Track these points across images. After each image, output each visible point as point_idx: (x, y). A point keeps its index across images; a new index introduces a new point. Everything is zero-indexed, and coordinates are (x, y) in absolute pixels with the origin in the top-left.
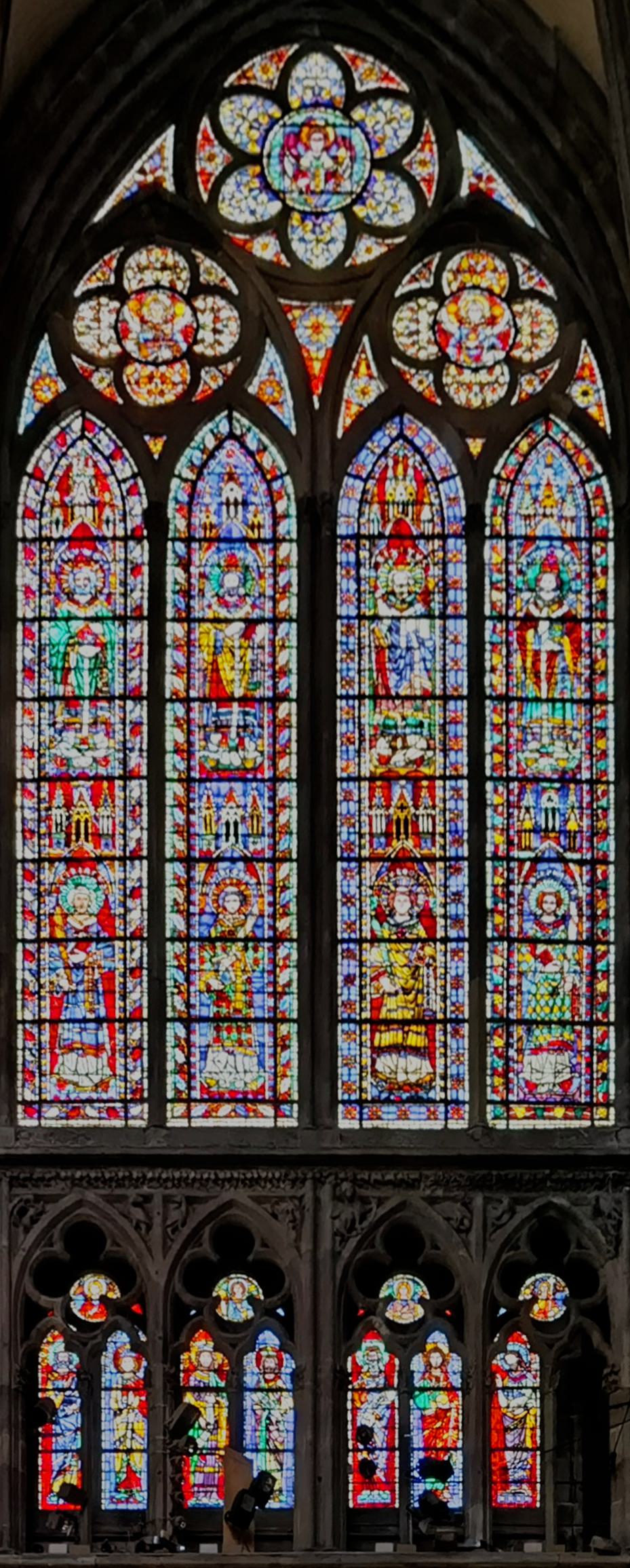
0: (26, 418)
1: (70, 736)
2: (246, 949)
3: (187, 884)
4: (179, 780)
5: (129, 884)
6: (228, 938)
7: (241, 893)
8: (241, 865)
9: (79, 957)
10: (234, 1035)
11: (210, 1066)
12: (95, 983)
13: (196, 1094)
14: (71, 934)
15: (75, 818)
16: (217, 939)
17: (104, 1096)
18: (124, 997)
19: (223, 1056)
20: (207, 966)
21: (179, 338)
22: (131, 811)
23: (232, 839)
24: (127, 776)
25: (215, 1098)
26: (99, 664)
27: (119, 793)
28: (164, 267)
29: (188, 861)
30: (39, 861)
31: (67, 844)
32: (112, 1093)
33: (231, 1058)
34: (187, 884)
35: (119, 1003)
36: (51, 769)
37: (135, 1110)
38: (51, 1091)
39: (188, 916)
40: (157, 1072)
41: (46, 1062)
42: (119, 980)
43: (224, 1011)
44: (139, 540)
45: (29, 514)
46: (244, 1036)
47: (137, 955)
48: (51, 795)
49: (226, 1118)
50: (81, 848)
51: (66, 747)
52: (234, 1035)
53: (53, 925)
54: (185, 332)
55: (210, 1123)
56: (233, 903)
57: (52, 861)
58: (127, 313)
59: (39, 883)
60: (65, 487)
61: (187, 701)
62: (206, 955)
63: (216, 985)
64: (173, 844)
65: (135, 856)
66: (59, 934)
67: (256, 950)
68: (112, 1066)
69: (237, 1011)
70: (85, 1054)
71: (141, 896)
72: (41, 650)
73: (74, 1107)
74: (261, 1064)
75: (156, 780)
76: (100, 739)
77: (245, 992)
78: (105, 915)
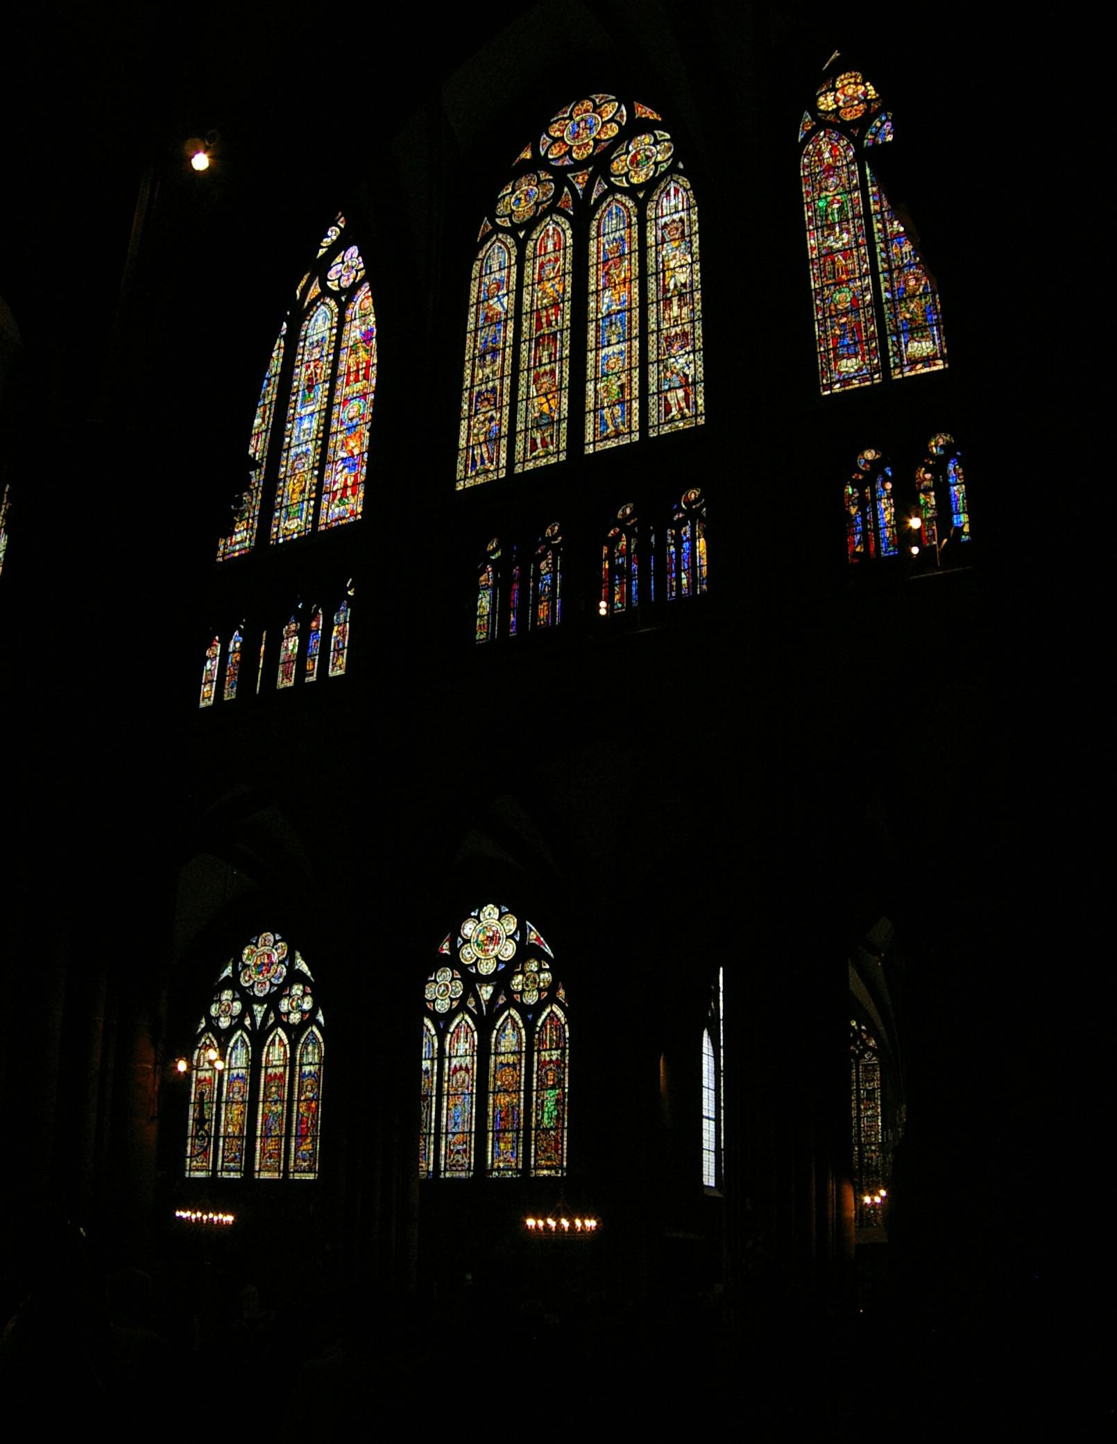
0: (800, 137)
1: (832, 238)
2: (920, 299)
3: (891, 280)
4: (882, 242)
5: (864, 286)
6: (912, 296)
7: (915, 278)
8: (914, 267)
9: (844, 320)
10: (920, 334)
11: (910, 350)
12: (852, 328)
13: (905, 363)
14: (839, 312)
15: (836, 267)
16: (906, 298)
17: (861, 373)
18: (866, 331)
19: (916, 344)
20: (904, 309)
21: (861, 96)
22: (861, 259)
23: (909, 258)
24: (858, 246)
25: (913, 362)
26: (841, 210)
27: (855, 253)
28: (851, 77)
29: (890, 271)
30: (822, 289)
31: (834, 277)
32: (865, 372)
33: (920, 344)
34: (891, 280)
35: (864, 334)
36: (824, 252)
37: (876, 376)
38: (836, 377)
39: (892, 292)
40: (885, 359)
41: (832, 366)
42: (863, 325)
43: (914, 326)
44: (853, 164)
45: (806, 167)
46: (925, 334)
47: (870, 313)
48: (825, 262)
49: (921, 370)
50: (840, 278)
51: (830, 242)
52: (920, 334)
53: (830, 311)
54: (863, 94)
55: (913, 373)
56: (912, 283)
57: (828, 286)
58: (838, 95)
59: (823, 295)
60: (820, 153)
61: (882, 213)
62: (903, 305)
63: (908, 316)
64: (882, 266)
65: (865, 275)
66: (834, 313)
67: (925, 298)
68: (863, 360)
69: (919, 324)
70: (850, 358)
71: (869, 290)
72: (816, 210)
73: (845, 381)
74: (934, 343)
75: (871, 245)
76: (845, 236)
77: (923, 316)
78: (854, 300)
